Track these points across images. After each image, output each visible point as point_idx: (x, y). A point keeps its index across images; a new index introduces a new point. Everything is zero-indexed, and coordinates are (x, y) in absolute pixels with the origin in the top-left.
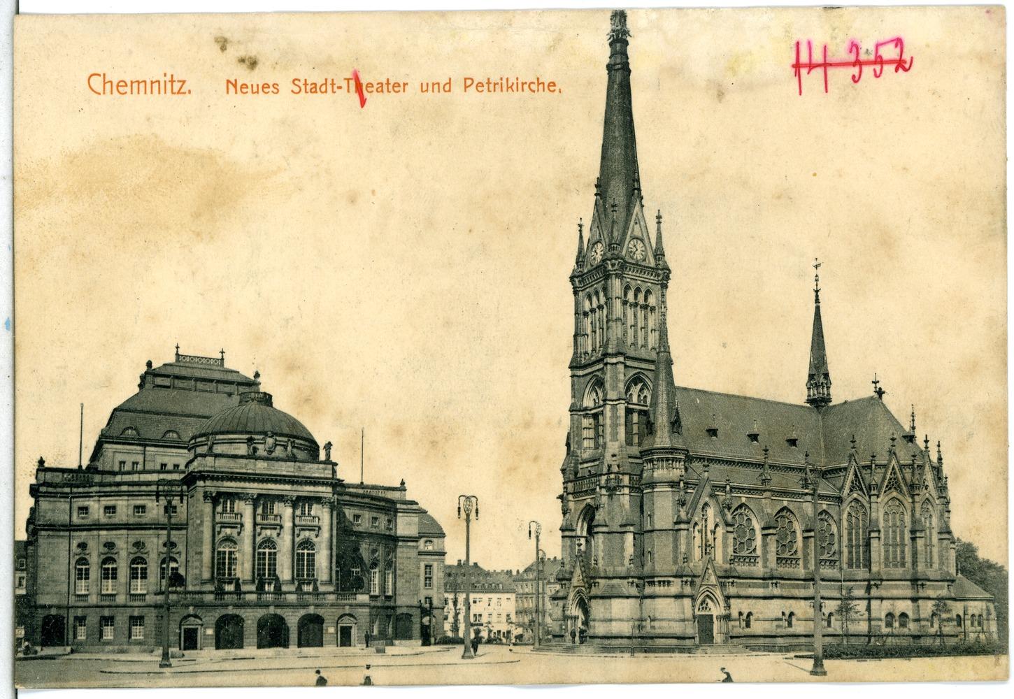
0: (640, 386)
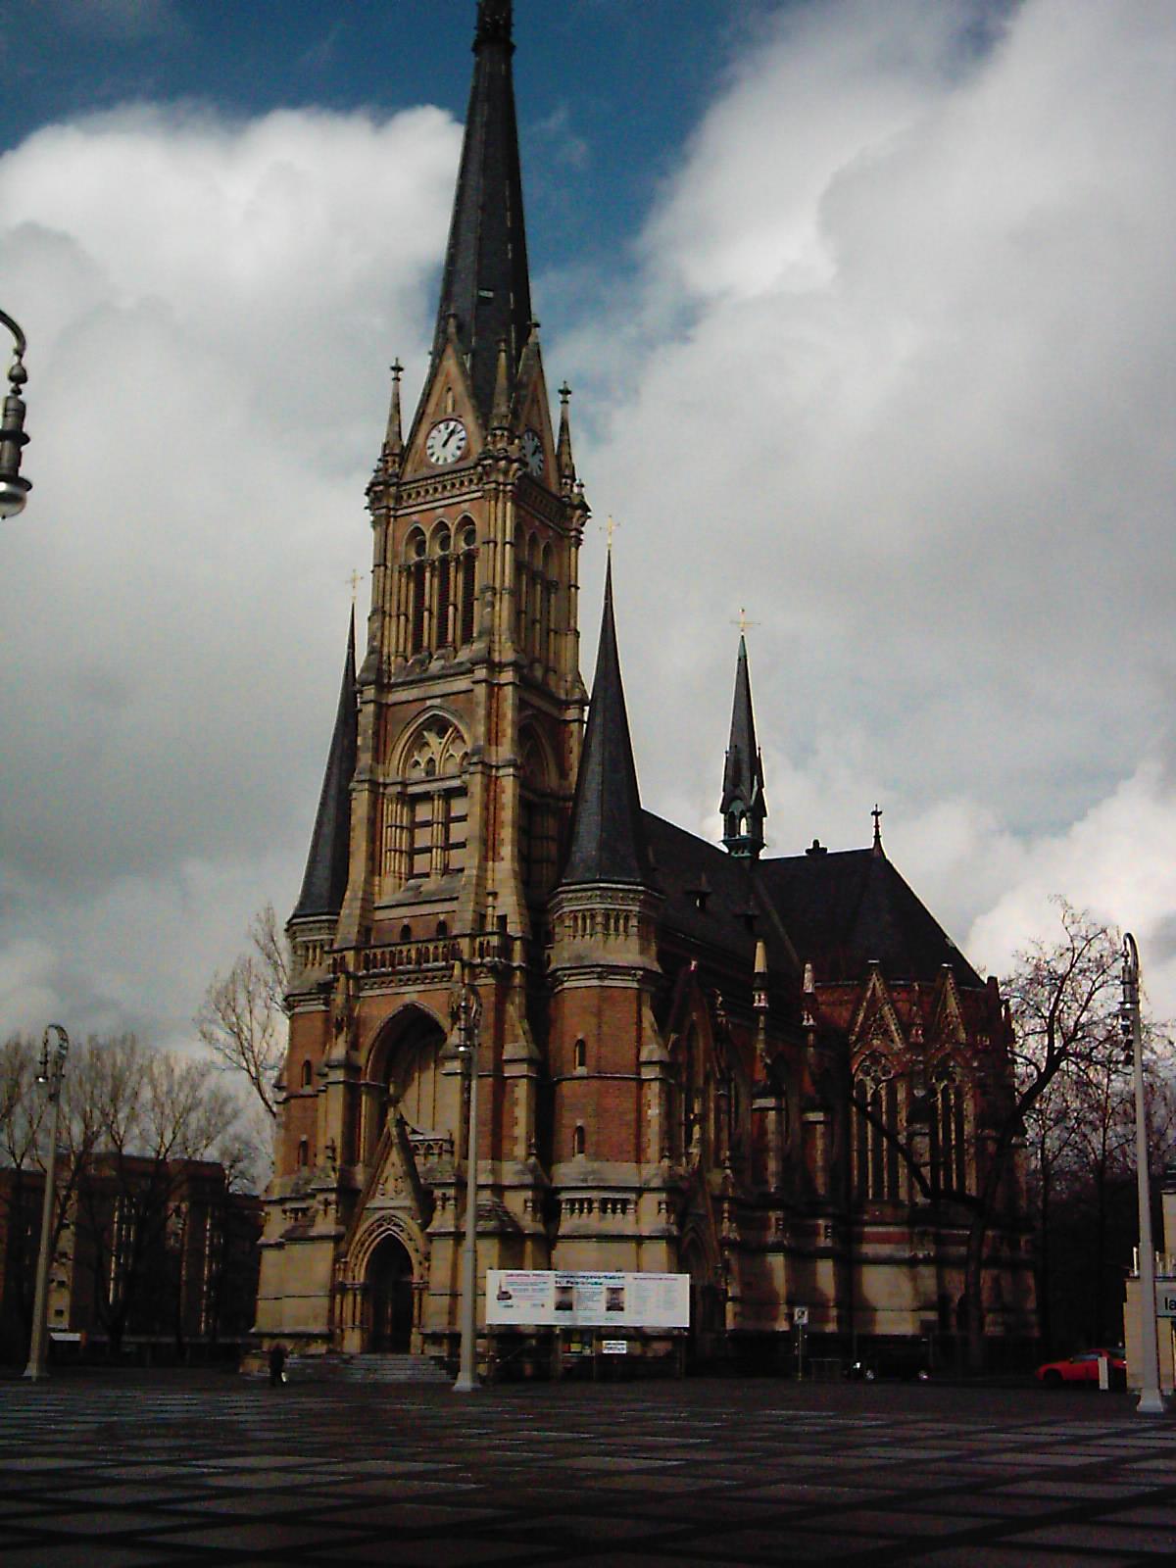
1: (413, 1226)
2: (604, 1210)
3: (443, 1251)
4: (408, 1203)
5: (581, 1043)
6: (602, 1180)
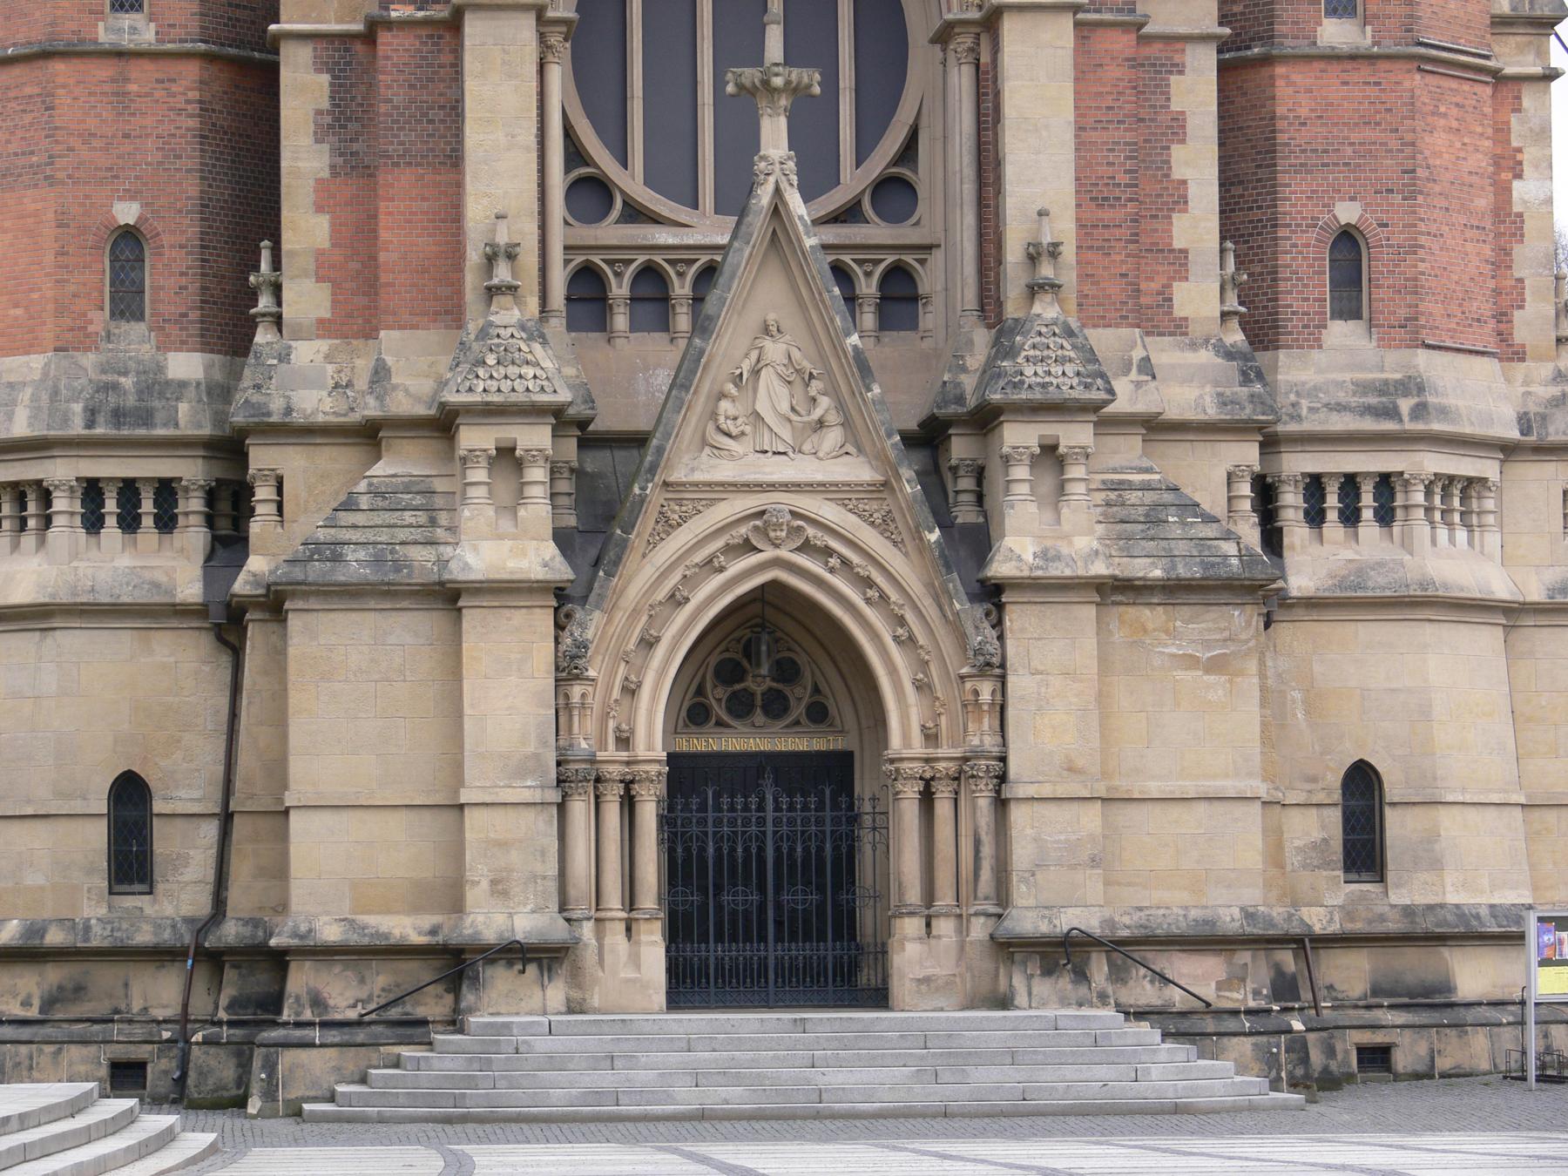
1: (905, 569)
3: (1050, 657)
4: (860, 471)
6: (1444, 412)
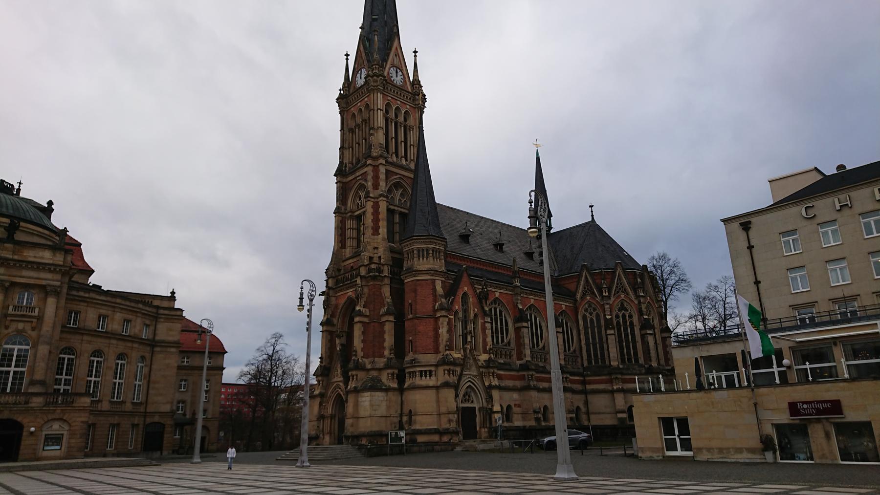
0: (400, 191)
2: (421, 376)
5: (411, 304)
